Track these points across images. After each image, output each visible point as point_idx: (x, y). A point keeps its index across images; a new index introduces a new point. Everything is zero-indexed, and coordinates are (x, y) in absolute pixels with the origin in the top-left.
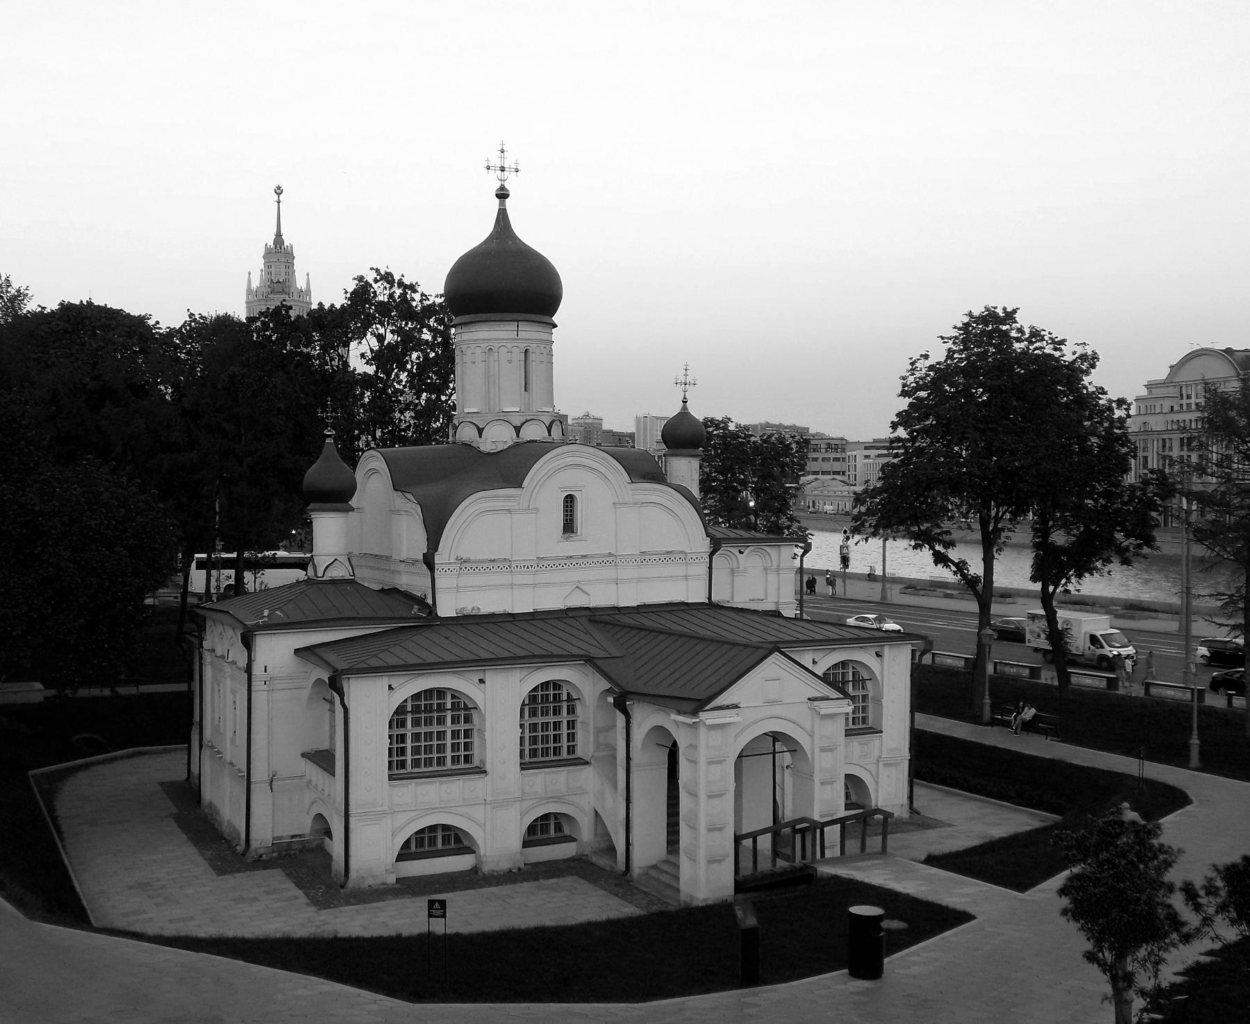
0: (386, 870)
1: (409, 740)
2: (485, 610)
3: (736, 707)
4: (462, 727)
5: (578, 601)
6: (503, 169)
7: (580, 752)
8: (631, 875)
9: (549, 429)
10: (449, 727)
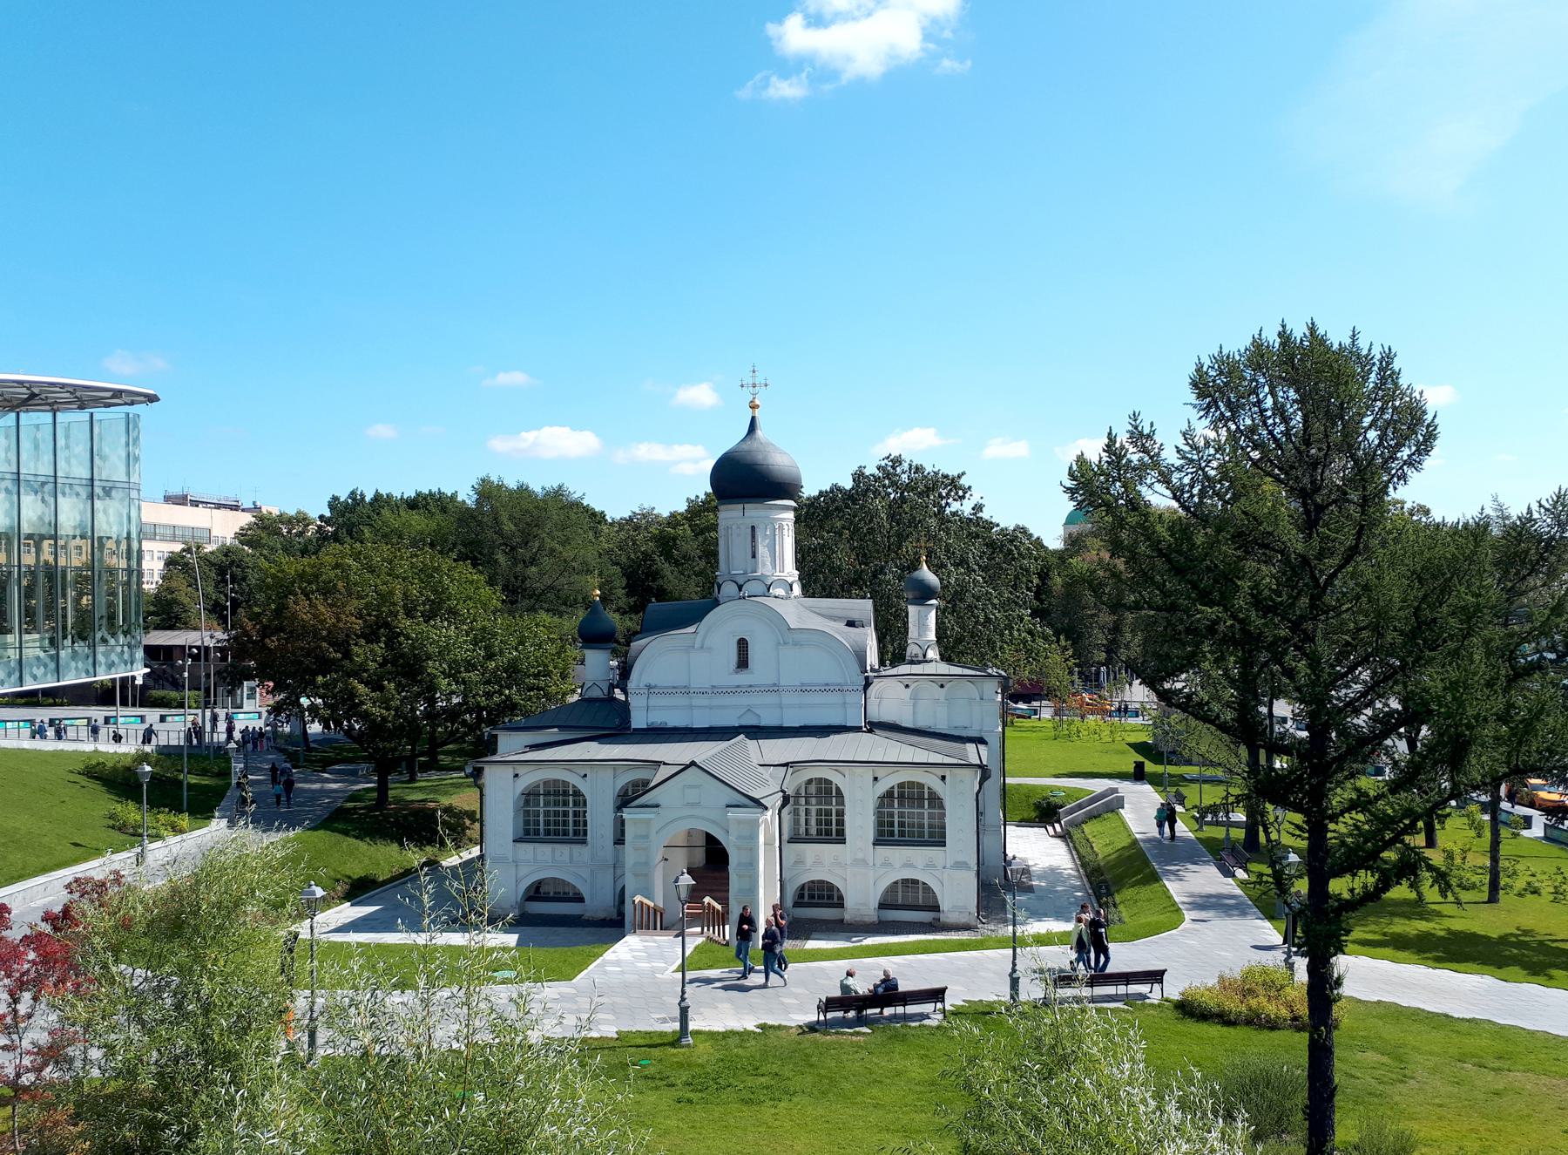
2: (671, 725)
6: (754, 386)
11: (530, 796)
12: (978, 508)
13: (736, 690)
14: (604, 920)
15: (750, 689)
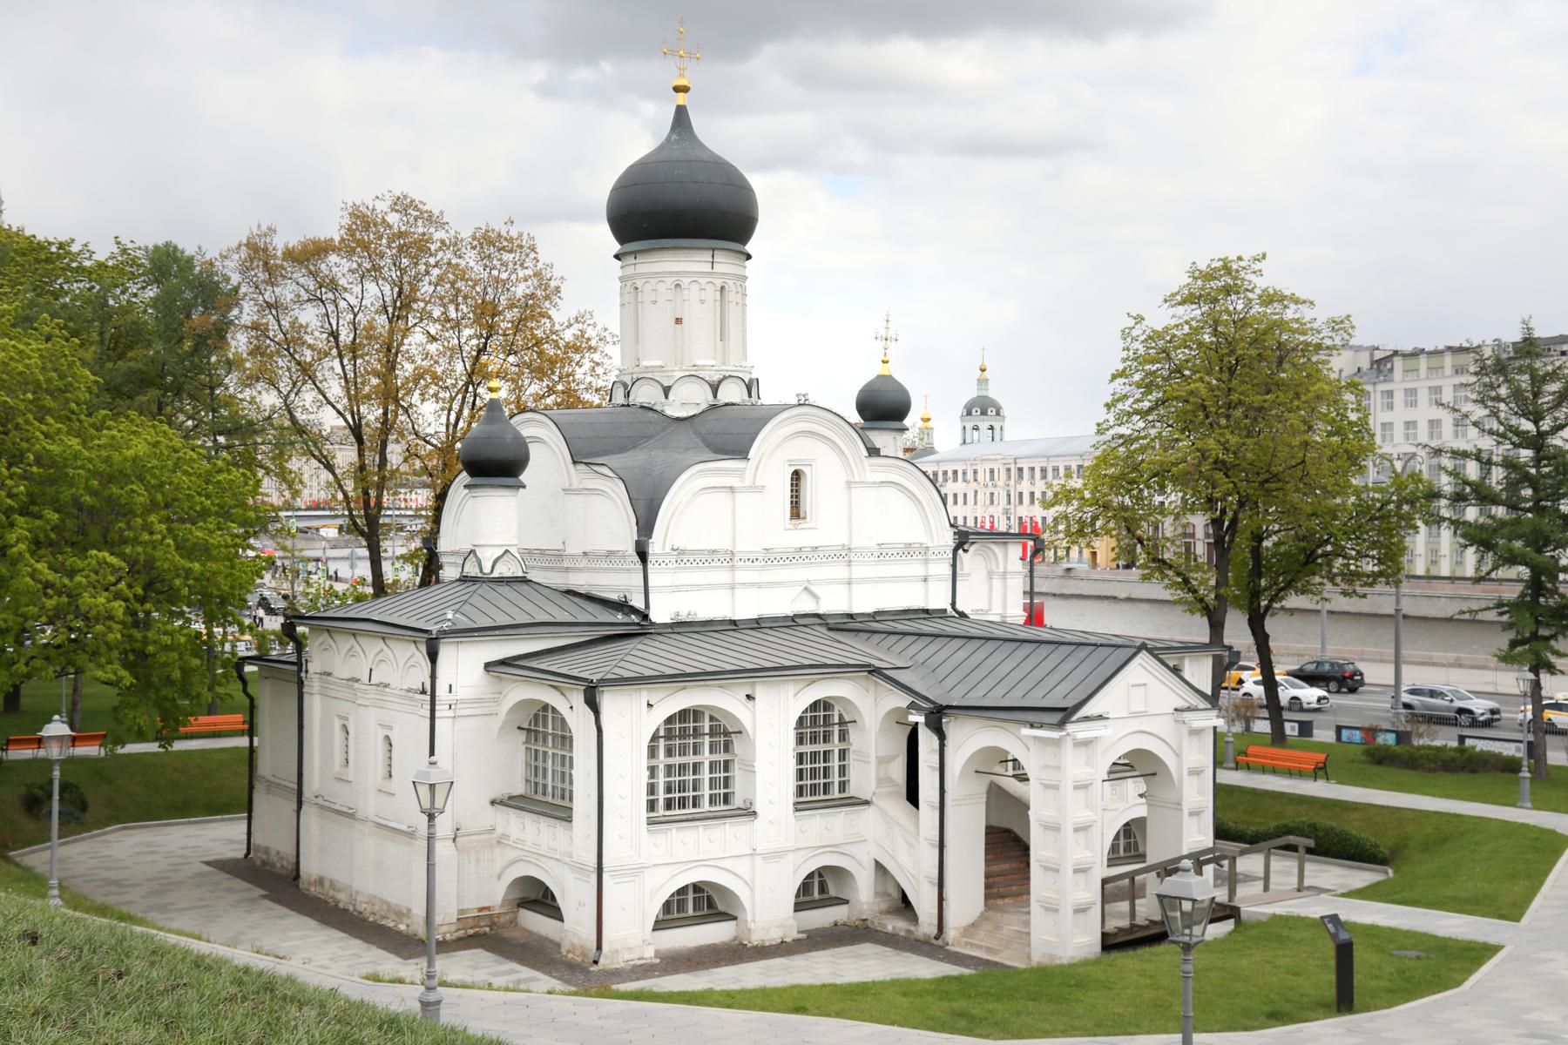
0: (644, 941)
2: (703, 615)
3: (1100, 717)
4: (721, 757)
5: (807, 606)
7: (853, 790)
8: (944, 939)
10: (706, 757)
13: (798, 555)
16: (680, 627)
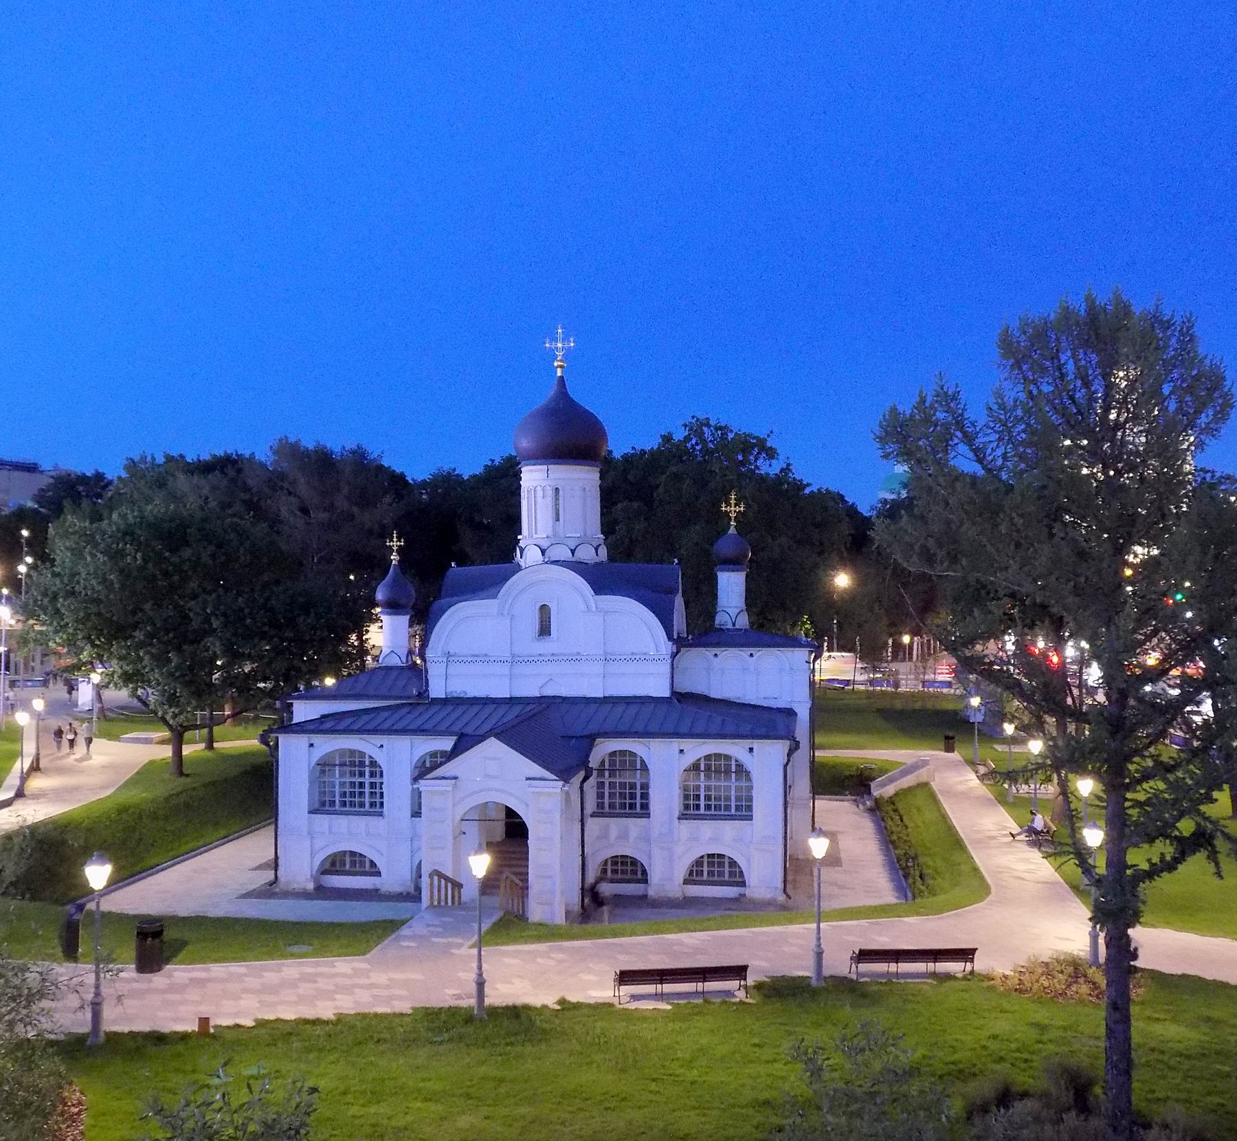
0: (307, 879)
1: (337, 787)
2: (470, 694)
9: (596, 550)
10: (367, 780)
11: (324, 766)
12: (787, 470)
14: (401, 894)
15: (554, 658)
16: (445, 702)
